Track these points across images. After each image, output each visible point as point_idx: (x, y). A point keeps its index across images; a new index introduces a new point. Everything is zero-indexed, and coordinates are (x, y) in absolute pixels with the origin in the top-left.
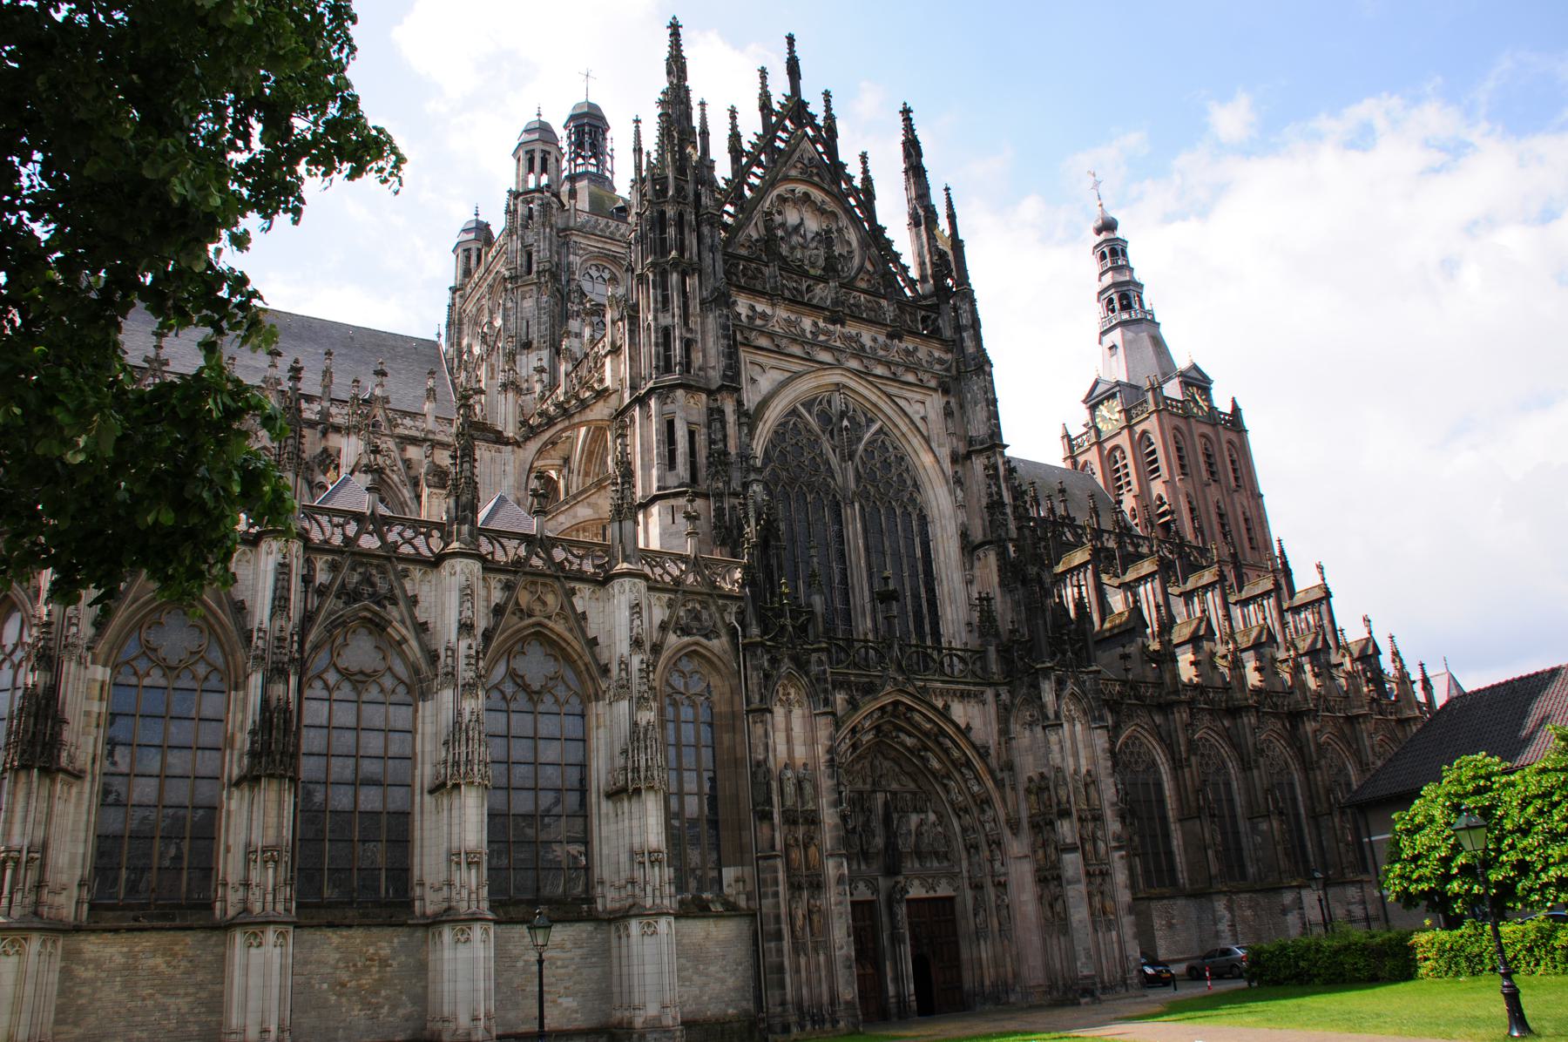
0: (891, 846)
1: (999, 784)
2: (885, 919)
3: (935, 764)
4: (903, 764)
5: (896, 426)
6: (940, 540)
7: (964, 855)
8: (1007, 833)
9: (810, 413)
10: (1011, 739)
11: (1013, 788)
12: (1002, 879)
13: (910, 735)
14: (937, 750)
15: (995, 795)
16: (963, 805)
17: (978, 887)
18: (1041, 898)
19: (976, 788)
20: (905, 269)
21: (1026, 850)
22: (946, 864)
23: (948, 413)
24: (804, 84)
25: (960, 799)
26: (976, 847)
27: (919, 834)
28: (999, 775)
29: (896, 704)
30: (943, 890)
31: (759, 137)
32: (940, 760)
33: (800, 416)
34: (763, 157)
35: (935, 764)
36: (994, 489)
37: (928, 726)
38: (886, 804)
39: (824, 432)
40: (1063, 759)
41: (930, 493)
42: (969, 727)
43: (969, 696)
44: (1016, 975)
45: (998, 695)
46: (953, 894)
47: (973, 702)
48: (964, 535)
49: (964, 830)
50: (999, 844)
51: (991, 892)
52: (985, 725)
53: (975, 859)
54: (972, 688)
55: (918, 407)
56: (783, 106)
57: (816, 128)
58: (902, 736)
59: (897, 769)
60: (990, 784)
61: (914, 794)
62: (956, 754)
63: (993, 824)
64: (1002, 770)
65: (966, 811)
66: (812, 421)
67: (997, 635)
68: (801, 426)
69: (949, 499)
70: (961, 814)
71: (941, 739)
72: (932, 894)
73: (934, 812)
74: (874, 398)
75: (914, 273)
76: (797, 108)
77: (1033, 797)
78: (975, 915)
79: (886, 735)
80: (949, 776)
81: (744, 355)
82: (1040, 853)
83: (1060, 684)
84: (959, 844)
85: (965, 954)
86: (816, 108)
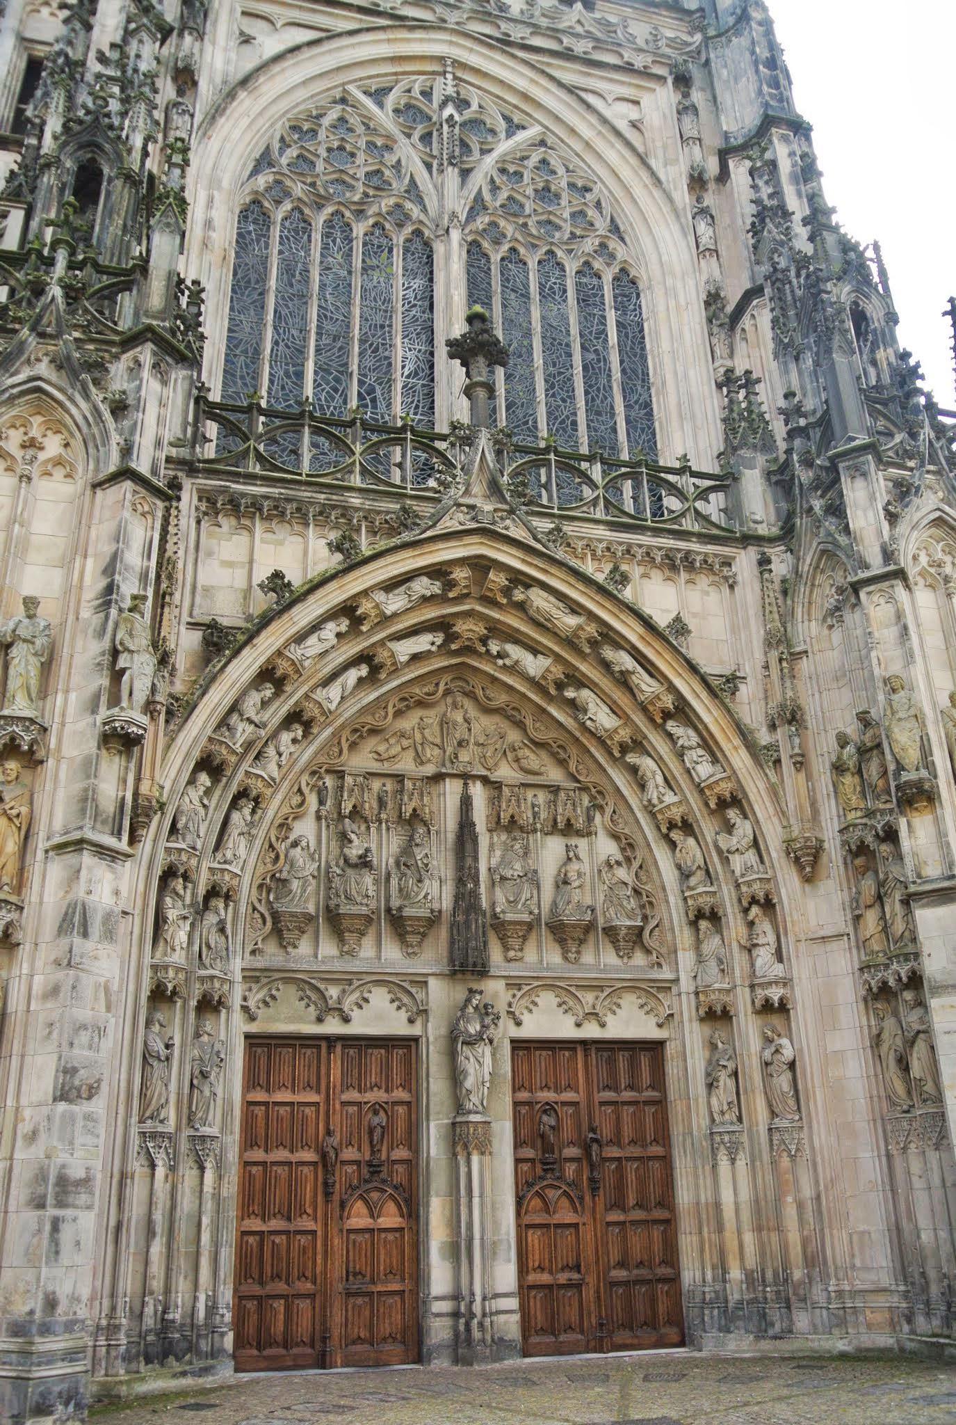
1: (764, 756)
2: (436, 1087)
3: (603, 718)
4: (529, 722)
5: (573, 131)
6: (662, 315)
7: (684, 936)
8: (788, 884)
10: (796, 656)
11: (801, 763)
12: (775, 994)
13: (535, 650)
14: (605, 683)
16: (676, 814)
17: (717, 1016)
18: (877, 1041)
19: (704, 770)
21: (838, 921)
22: (639, 959)
23: (686, 109)
25: (670, 798)
26: (714, 917)
27: (563, 882)
28: (764, 737)
29: (481, 565)
32: (615, 710)
35: (603, 718)
36: (766, 191)
37: (572, 621)
38: (466, 803)
40: (909, 658)
41: (646, 242)
42: (680, 627)
43: (690, 566)
44: (814, 1260)
45: (764, 562)
46: (654, 1033)
47: (703, 581)
48: (713, 299)
49: (685, 875)
50: (768, 905)
51: (749, 1028)
52: (734, 630)
53: (712, 944)
54: (695, 546)
55: (624, 108)
58: (515, 652)
59: (514, 736)
60: (740, 759)
61: (555, 790)
62: (647, 685)
63: (751, 856)
64: (773, 727)
65: (687, 827)
66: (384, 118)
67: (767, 444)
69: (682, 244)
70: (676, 835)
71: (608, 653)
72: (591, 1031)
73: (615, 837)
74: (521, 83)
77: (849, 780)
78: (711, 1086)
79: (468, 650)
80: (638, 744)
82: (871, 919)
83: (903, 492)
84: (674, 911)
85: (684, 1196)
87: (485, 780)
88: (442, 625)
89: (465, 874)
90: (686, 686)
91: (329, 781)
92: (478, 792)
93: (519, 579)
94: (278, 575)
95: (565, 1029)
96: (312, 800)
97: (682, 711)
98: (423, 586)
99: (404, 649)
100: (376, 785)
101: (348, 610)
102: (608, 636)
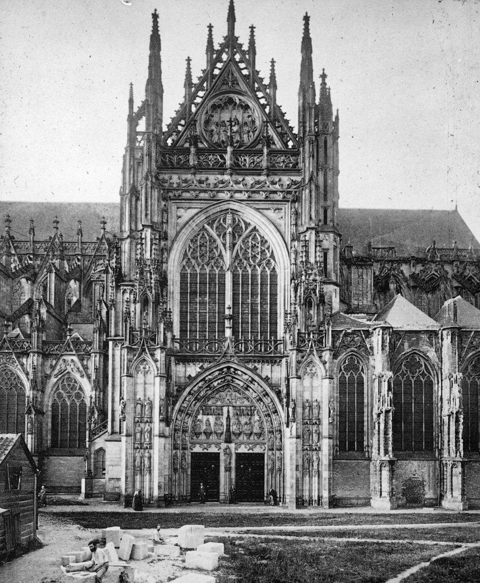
0: (228, 430)
9: (212, 228)
15: (279, 407)
20: (291, 128)
24: (237, 25)
30: (257, 450)
31: (204, 71)
33: (206, 230)
34: (205, 85)
38: (228, 411)
39: (219, 236)
50: (280, 431)
56: (221, 45)
57: (243, 53)
58: (237, 381)
68: (206, 235)
75: (296, 131)
76: (231, 41)
81: (173, 207)
86: (244, 40)
87: (233, 406)
88: (224, 377)
89: (228, 426)
90: (268, 390)
91: (204, 407)
92: (231, 408)
93: (236, 369)
94: (190, 376)
95: (246, 451)
96: (201, 411)
97: (267, 394)
98: (217, 373)
99: (215, 384)
100: (212, 408)
101: (204, 379)
102: (253, 380)
